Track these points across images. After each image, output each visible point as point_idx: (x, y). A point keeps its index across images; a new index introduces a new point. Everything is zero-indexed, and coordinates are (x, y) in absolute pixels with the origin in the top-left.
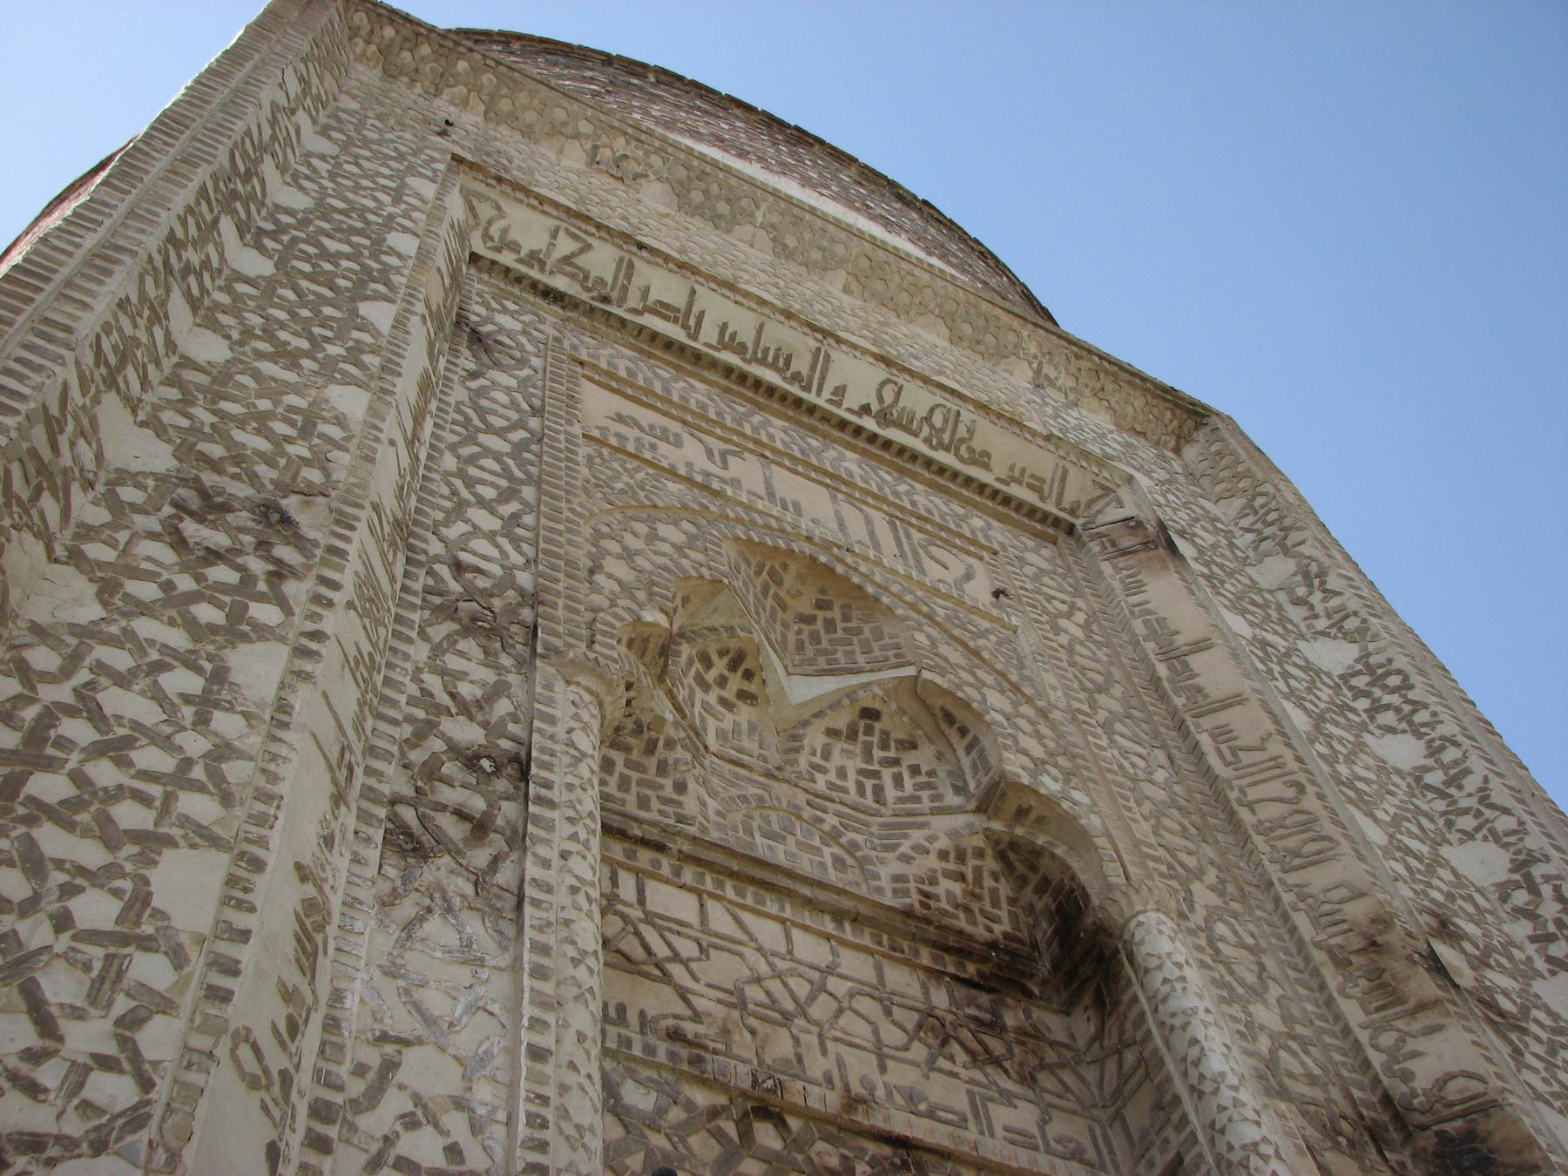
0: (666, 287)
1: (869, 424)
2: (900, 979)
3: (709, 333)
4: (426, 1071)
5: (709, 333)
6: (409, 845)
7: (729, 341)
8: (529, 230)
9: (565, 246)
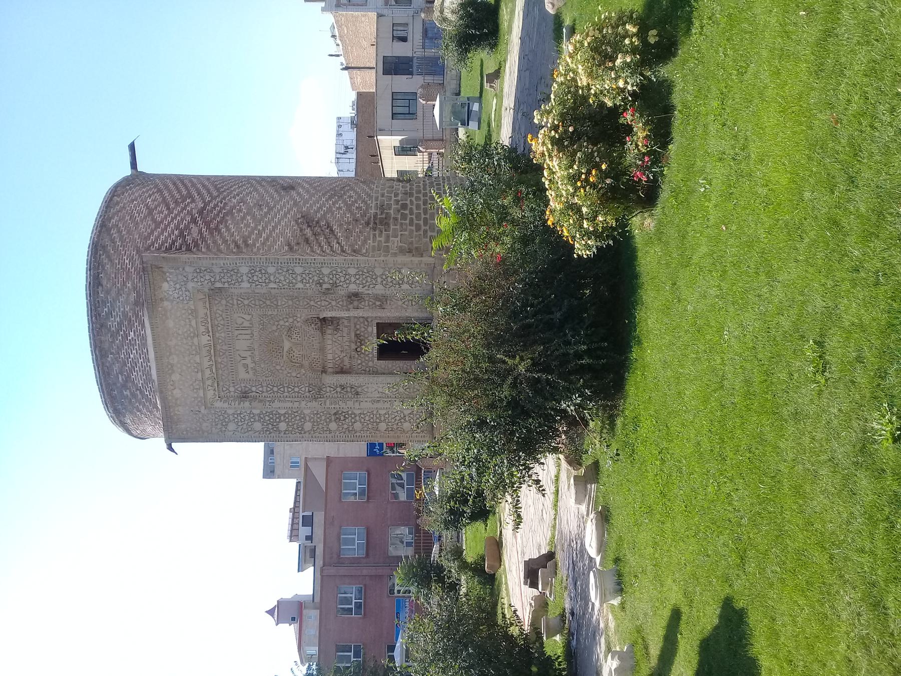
0: (208, 372)
1: (211, 334)
2: (329, 331)
3: (211, 363)
4: (380, 390)
5: (211, 363)
6: (357, 394)
7: (210, 359)
8: (210, 394)
9: (210, 388)
